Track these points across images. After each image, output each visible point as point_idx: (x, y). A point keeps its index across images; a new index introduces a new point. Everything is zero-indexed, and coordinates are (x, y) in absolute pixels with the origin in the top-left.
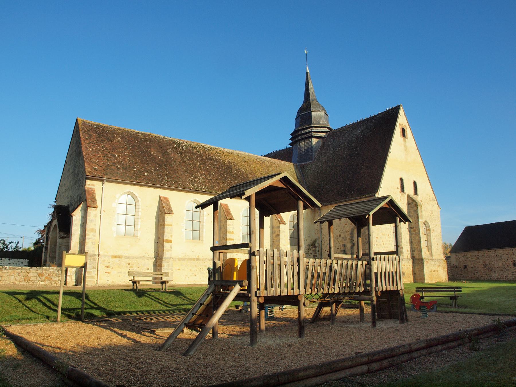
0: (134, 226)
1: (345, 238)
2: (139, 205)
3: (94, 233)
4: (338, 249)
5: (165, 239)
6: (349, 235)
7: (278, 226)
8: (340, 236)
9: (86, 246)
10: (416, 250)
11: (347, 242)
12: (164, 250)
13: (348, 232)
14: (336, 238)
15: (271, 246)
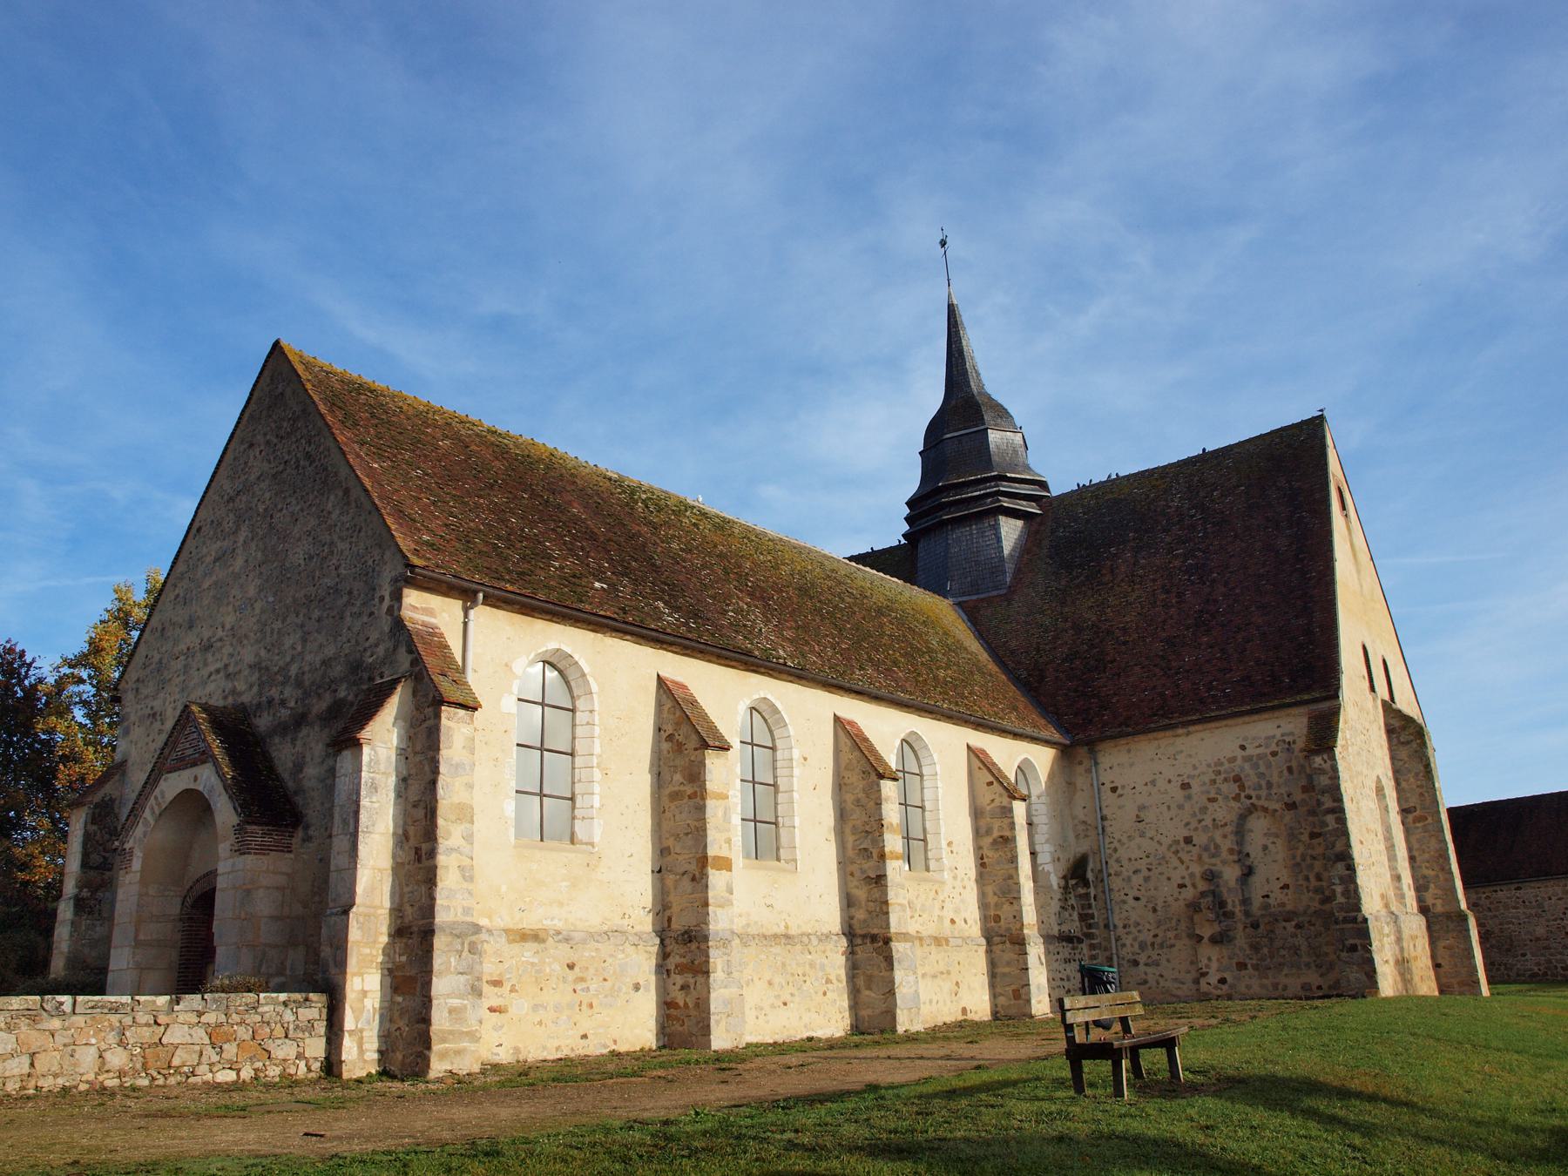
0: (572, 799)
1: (1213, 850)
2: (591, 711)
3: (468, 825)
4: (1181, 886)
5: (711, 852)
6: (1231, 837)
7: (1004, 807)
8: (1188, 840)
9: (440, 885)
10: (1432, 885)
11: (1224, 862)
13: (1226, 824)
14: (1173, 849)
15: (977, 881)
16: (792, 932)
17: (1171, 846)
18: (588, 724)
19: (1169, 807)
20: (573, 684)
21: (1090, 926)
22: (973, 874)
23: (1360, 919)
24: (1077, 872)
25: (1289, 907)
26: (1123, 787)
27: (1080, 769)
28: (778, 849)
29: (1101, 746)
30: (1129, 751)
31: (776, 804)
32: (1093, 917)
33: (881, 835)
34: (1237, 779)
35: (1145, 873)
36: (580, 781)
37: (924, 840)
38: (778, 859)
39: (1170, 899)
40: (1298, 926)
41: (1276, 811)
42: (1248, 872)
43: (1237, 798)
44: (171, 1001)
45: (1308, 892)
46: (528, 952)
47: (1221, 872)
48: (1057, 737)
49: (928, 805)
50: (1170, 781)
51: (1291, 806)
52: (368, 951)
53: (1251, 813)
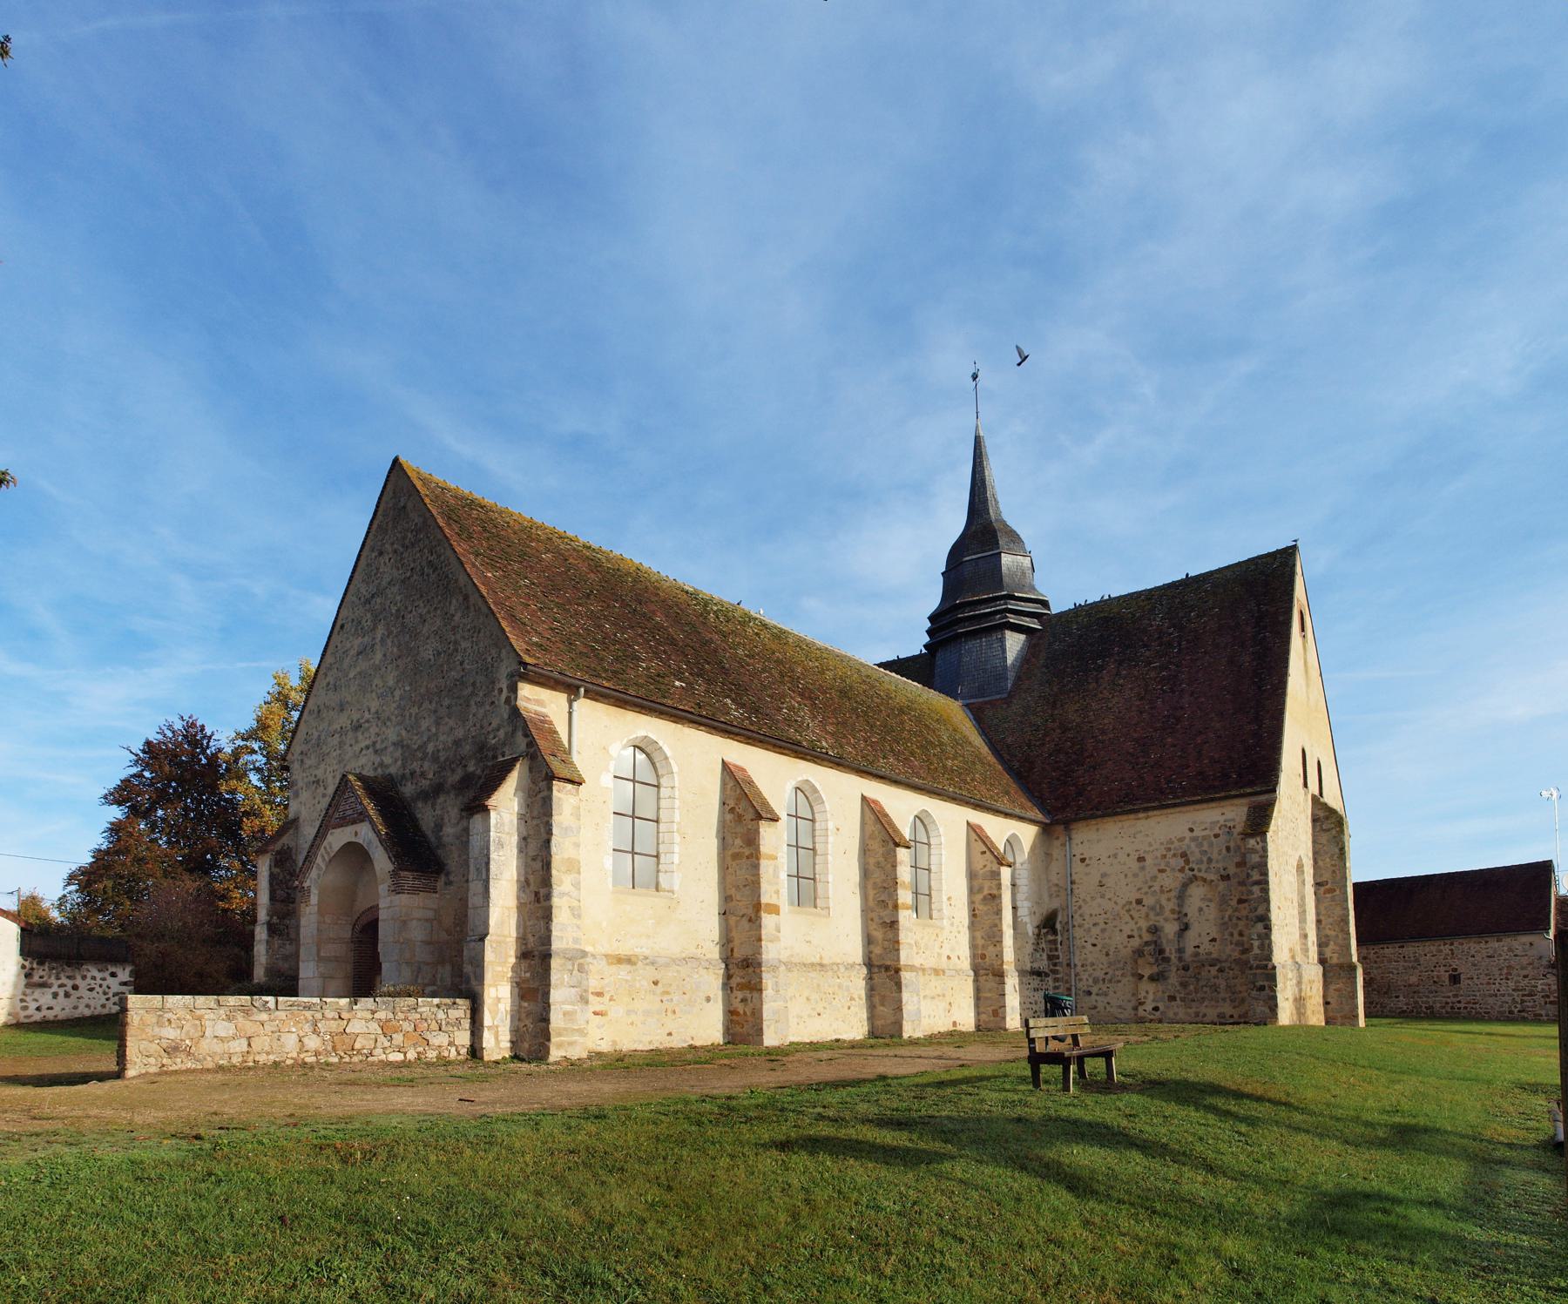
0: (657, 856)
3: (576, 875)
4: (1129, 937)
5: (764, 900)
8: (1139, 902)
10: (1332, 943)
11: (1166, 920)
12: (763, 937)
13: (1171, 890)
14: (1127, 907)
16: (824, 962)
17: (1125, 905)
18: (670, 797)
19: (1126, 876)
20: (658, 765)
21: (1055, 965)
22: (966, 922)
23: (1270, 967)
24: (1048, 923)
25: (1214, 956)
26: (1090, 858)
27: (1057, 843)
28: (815, 899)
29: (1074, 826)
30: (1098, 830)
31: (814, 864)
32: (1058, 957)
33: (896, 890)
34: (1184, 855)
35: (1102, 925)
36: (663, 842)
37: (930, 895)
38: (815, 907)
39: (1120, 947)
40: (1221, 970)
41: (1212, 881)
42: (1185, 928)
43: (1182, 870)
44: (351, 1002)
45: (1231, 943)
46: (623, 972)
47: (1163, 927)
48: (1040, 817)
49: (933, 868)
50: (1128, 855)
51: (1225, 878)
52: (500, 969)
53: (1192, 882)
